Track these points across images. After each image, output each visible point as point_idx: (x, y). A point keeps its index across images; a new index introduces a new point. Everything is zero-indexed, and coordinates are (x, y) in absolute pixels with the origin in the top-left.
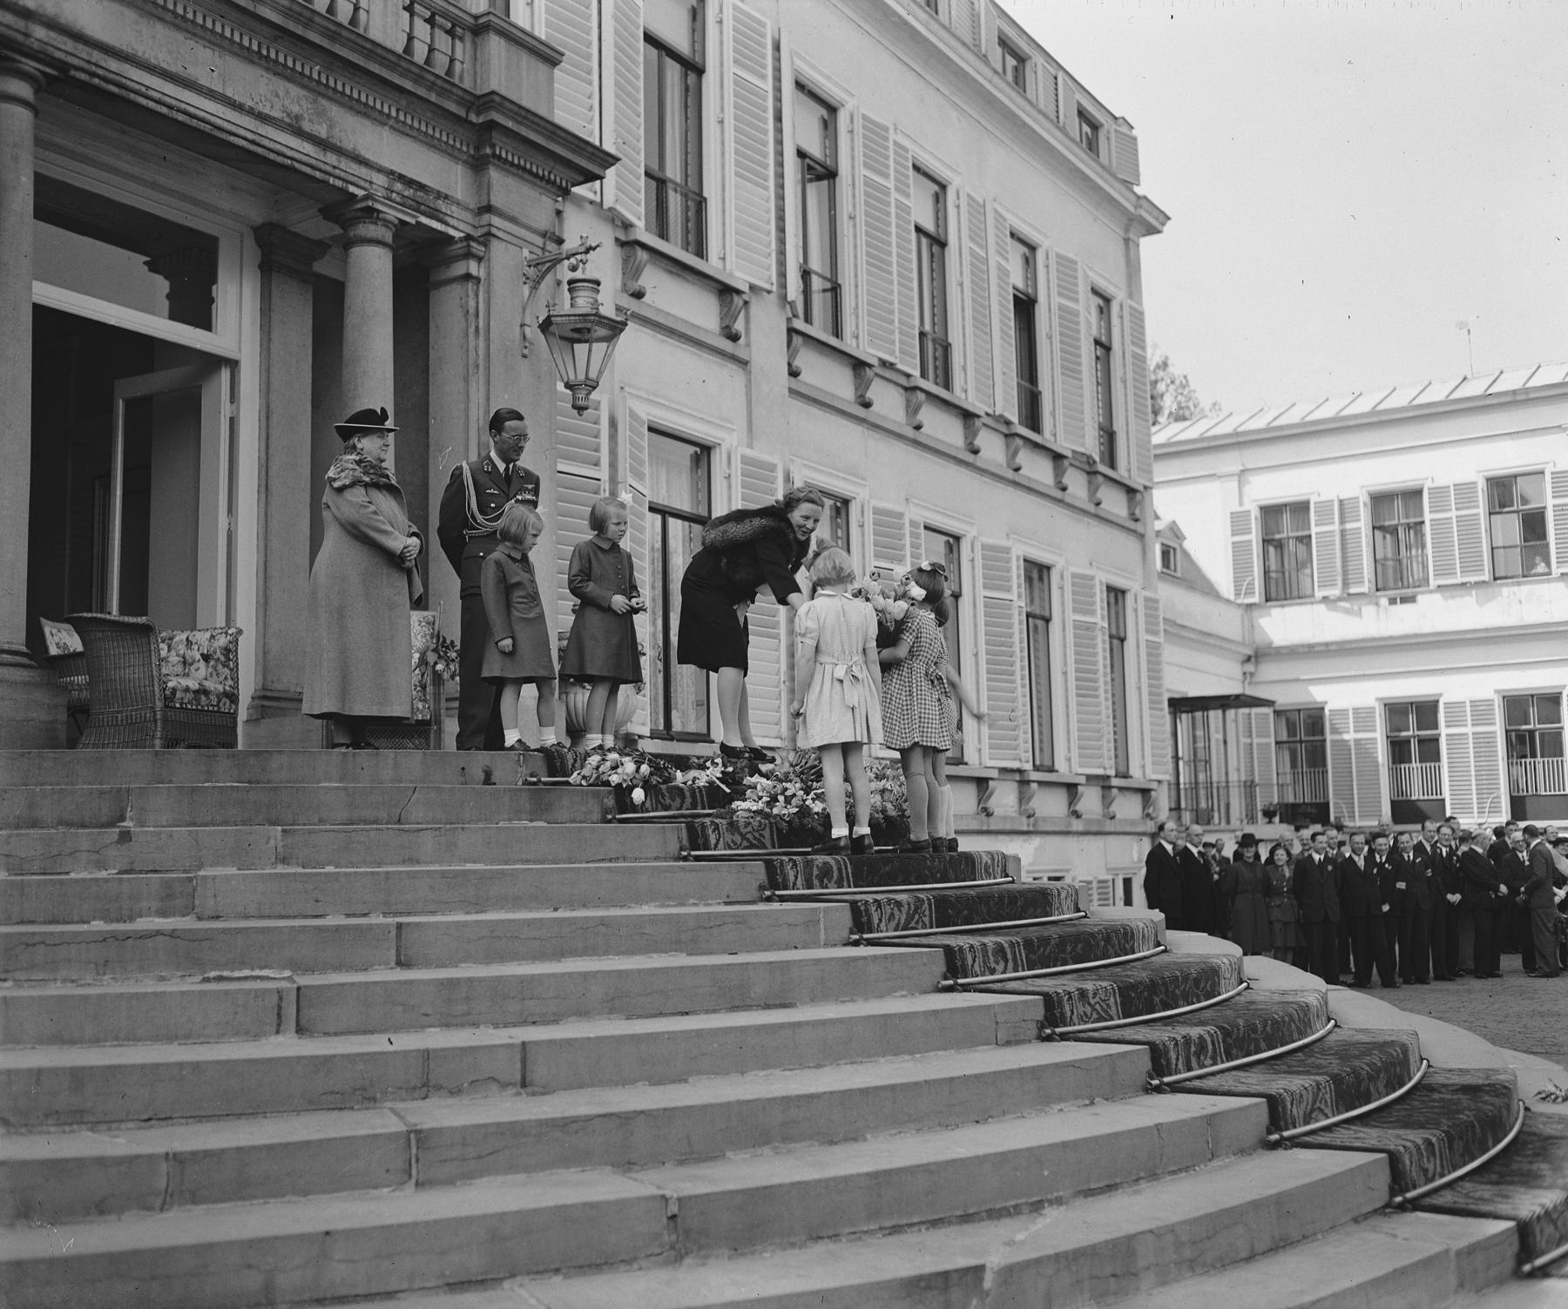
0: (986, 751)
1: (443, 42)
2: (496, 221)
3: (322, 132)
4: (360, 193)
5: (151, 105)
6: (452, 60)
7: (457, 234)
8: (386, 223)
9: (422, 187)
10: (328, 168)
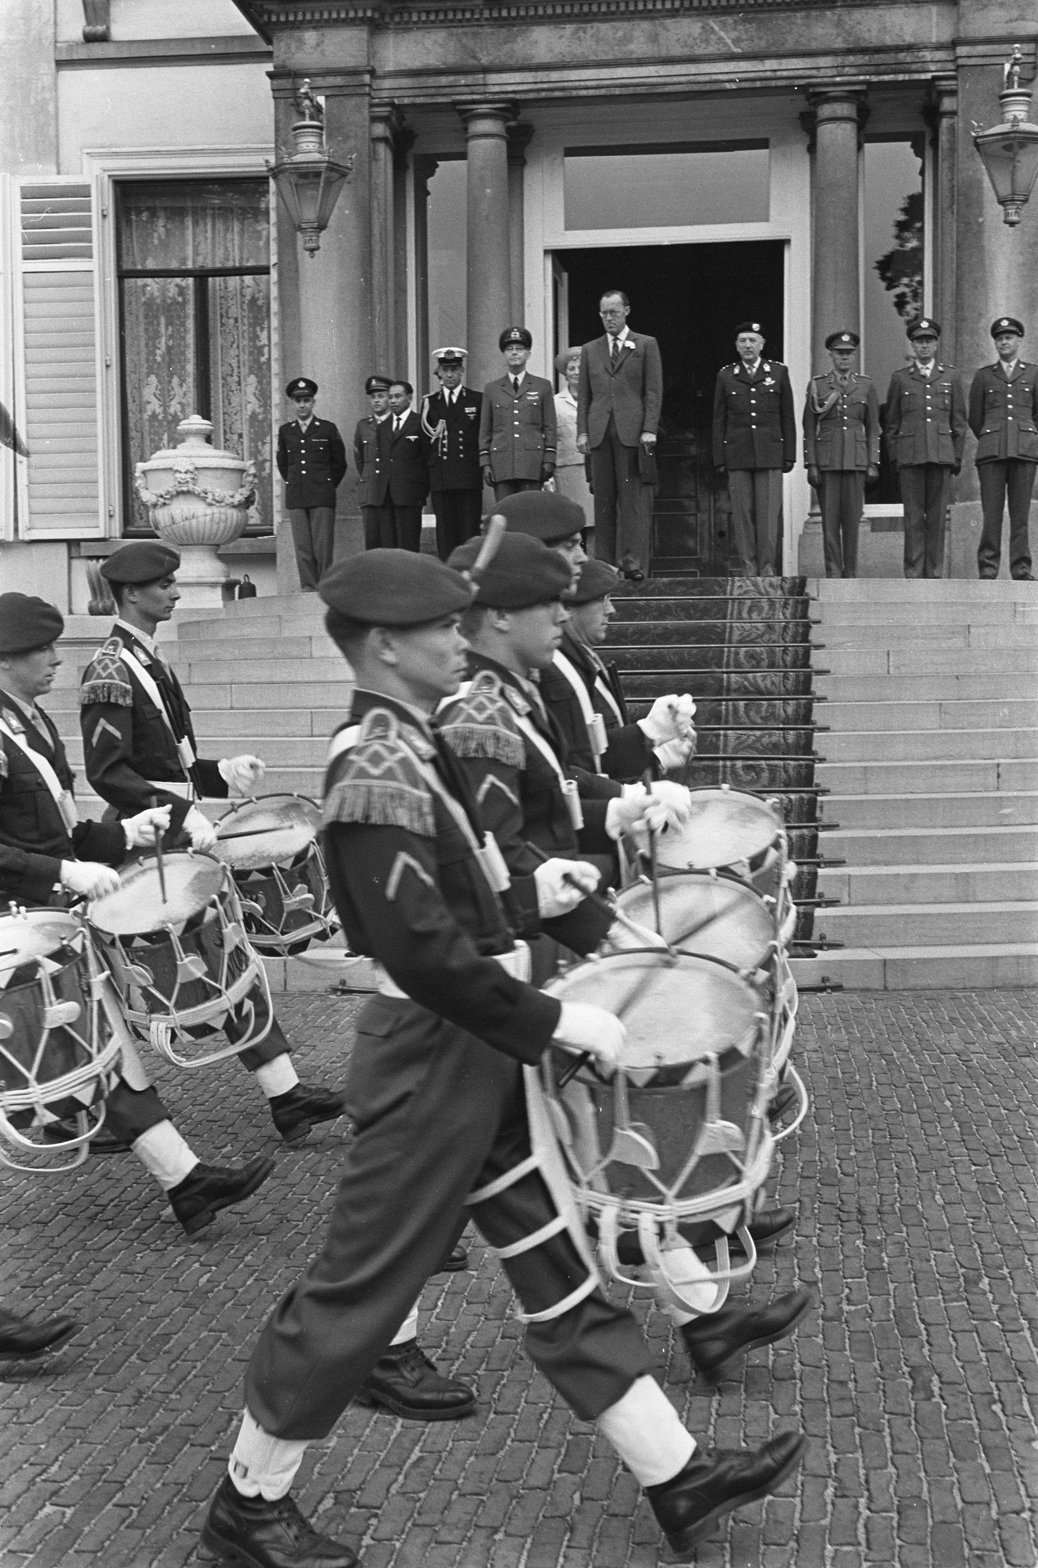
2: (962, 50)
5: (591, 92)
7: (929, 76)
10: (769, 74)
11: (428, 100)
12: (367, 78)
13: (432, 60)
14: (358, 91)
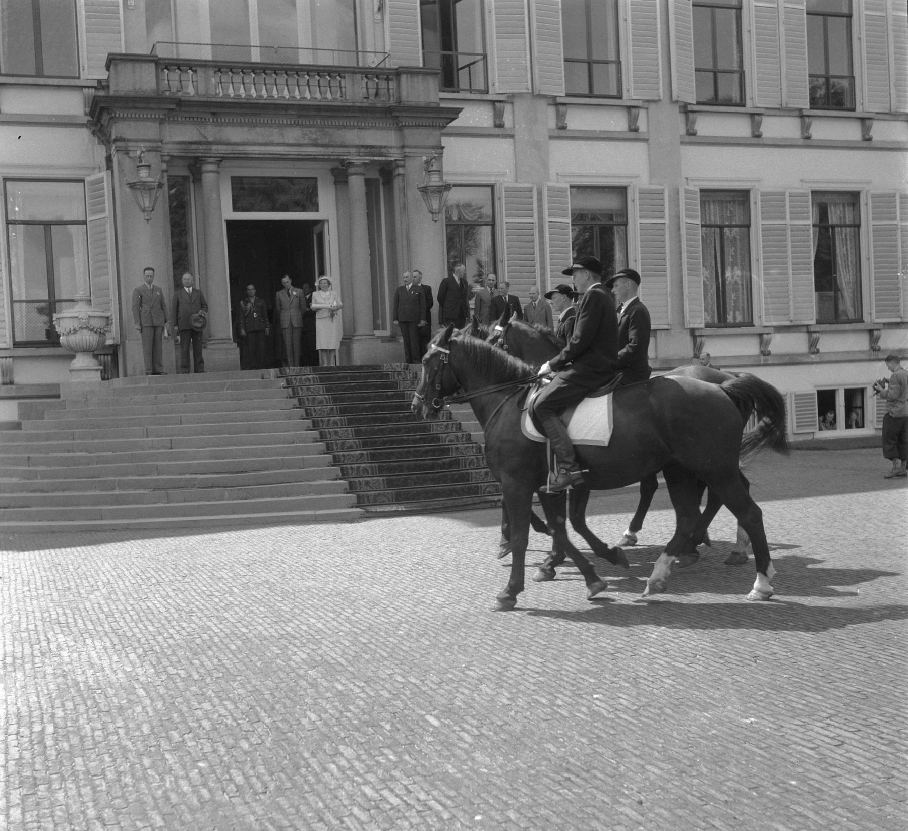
0: (874, 315)
1: (383, 85)
2: (407, 150)
3: (327, 141)
6: (389, 90)
7: (393, 159)
8: (357, 166)
9: (373, 147)
12: (160, 144)
13: (186, 139)
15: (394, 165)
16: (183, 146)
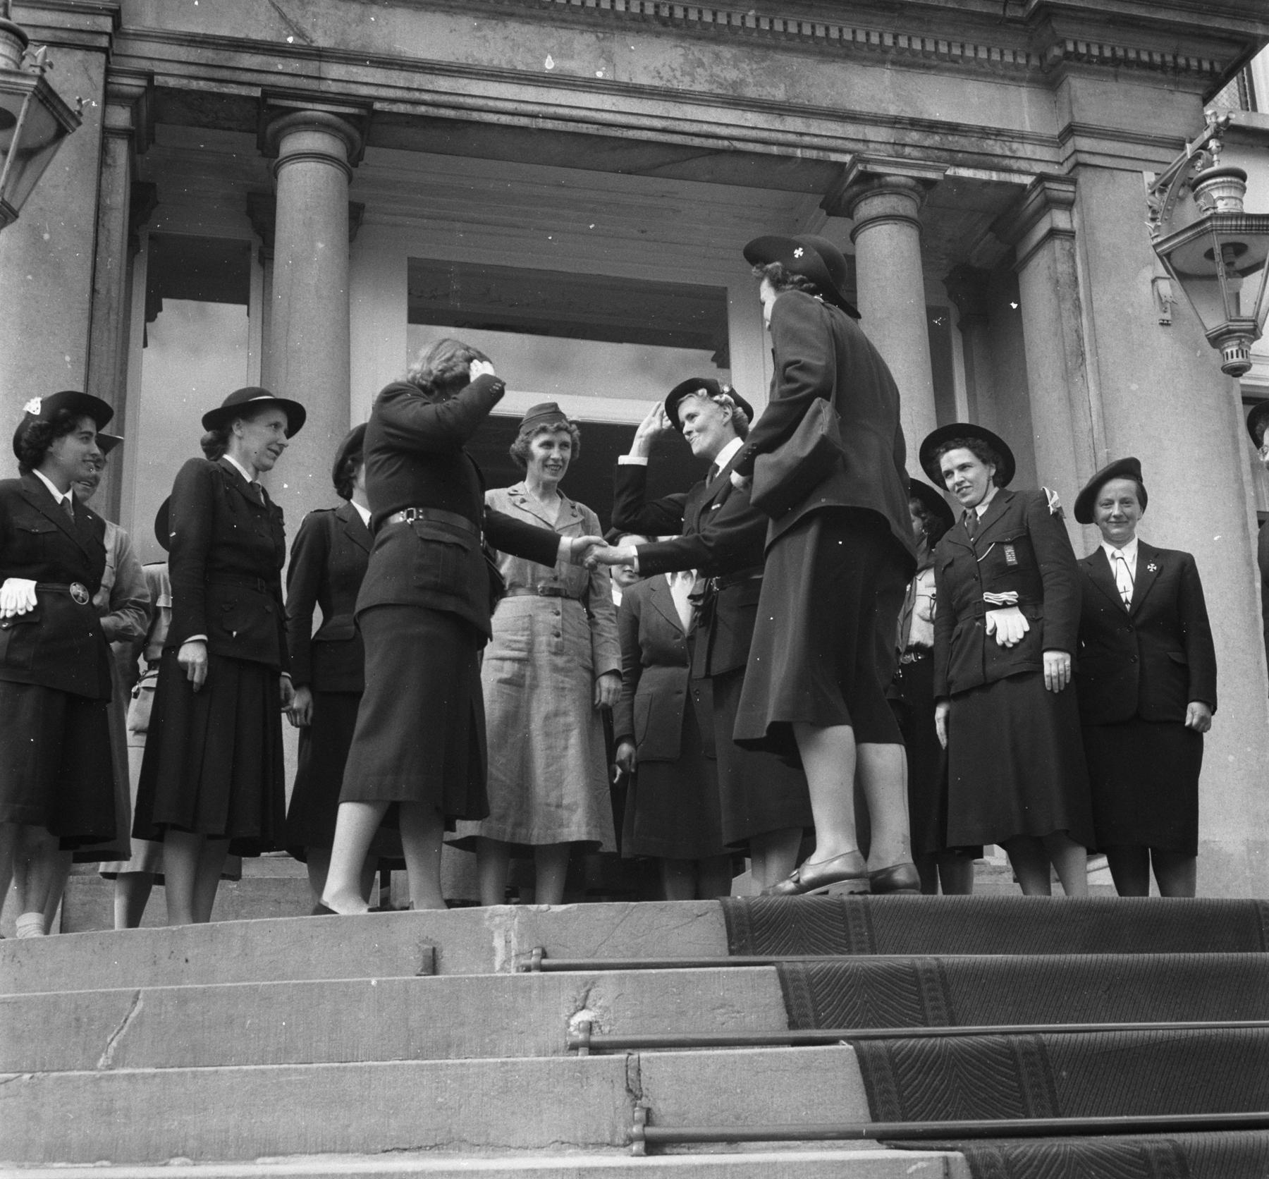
2: (1084, 143)
4: (847, 158)
5: (505, 119)
7: (1027, 180)
10: (791, 138)
11: (214, 87)
12: (106, 24)
14: (86, 39)
15: (1034, 200)
16: (207, 55)
